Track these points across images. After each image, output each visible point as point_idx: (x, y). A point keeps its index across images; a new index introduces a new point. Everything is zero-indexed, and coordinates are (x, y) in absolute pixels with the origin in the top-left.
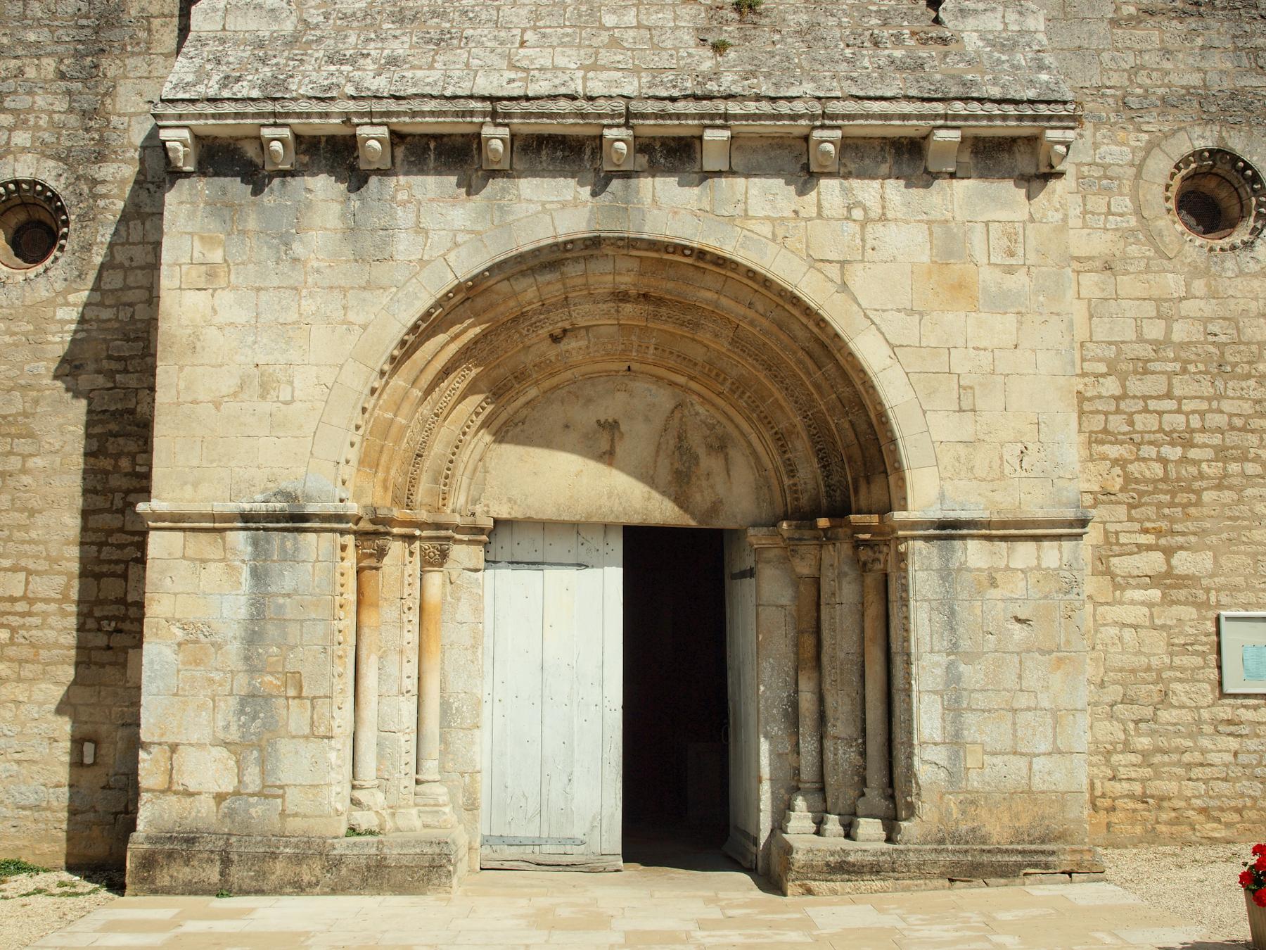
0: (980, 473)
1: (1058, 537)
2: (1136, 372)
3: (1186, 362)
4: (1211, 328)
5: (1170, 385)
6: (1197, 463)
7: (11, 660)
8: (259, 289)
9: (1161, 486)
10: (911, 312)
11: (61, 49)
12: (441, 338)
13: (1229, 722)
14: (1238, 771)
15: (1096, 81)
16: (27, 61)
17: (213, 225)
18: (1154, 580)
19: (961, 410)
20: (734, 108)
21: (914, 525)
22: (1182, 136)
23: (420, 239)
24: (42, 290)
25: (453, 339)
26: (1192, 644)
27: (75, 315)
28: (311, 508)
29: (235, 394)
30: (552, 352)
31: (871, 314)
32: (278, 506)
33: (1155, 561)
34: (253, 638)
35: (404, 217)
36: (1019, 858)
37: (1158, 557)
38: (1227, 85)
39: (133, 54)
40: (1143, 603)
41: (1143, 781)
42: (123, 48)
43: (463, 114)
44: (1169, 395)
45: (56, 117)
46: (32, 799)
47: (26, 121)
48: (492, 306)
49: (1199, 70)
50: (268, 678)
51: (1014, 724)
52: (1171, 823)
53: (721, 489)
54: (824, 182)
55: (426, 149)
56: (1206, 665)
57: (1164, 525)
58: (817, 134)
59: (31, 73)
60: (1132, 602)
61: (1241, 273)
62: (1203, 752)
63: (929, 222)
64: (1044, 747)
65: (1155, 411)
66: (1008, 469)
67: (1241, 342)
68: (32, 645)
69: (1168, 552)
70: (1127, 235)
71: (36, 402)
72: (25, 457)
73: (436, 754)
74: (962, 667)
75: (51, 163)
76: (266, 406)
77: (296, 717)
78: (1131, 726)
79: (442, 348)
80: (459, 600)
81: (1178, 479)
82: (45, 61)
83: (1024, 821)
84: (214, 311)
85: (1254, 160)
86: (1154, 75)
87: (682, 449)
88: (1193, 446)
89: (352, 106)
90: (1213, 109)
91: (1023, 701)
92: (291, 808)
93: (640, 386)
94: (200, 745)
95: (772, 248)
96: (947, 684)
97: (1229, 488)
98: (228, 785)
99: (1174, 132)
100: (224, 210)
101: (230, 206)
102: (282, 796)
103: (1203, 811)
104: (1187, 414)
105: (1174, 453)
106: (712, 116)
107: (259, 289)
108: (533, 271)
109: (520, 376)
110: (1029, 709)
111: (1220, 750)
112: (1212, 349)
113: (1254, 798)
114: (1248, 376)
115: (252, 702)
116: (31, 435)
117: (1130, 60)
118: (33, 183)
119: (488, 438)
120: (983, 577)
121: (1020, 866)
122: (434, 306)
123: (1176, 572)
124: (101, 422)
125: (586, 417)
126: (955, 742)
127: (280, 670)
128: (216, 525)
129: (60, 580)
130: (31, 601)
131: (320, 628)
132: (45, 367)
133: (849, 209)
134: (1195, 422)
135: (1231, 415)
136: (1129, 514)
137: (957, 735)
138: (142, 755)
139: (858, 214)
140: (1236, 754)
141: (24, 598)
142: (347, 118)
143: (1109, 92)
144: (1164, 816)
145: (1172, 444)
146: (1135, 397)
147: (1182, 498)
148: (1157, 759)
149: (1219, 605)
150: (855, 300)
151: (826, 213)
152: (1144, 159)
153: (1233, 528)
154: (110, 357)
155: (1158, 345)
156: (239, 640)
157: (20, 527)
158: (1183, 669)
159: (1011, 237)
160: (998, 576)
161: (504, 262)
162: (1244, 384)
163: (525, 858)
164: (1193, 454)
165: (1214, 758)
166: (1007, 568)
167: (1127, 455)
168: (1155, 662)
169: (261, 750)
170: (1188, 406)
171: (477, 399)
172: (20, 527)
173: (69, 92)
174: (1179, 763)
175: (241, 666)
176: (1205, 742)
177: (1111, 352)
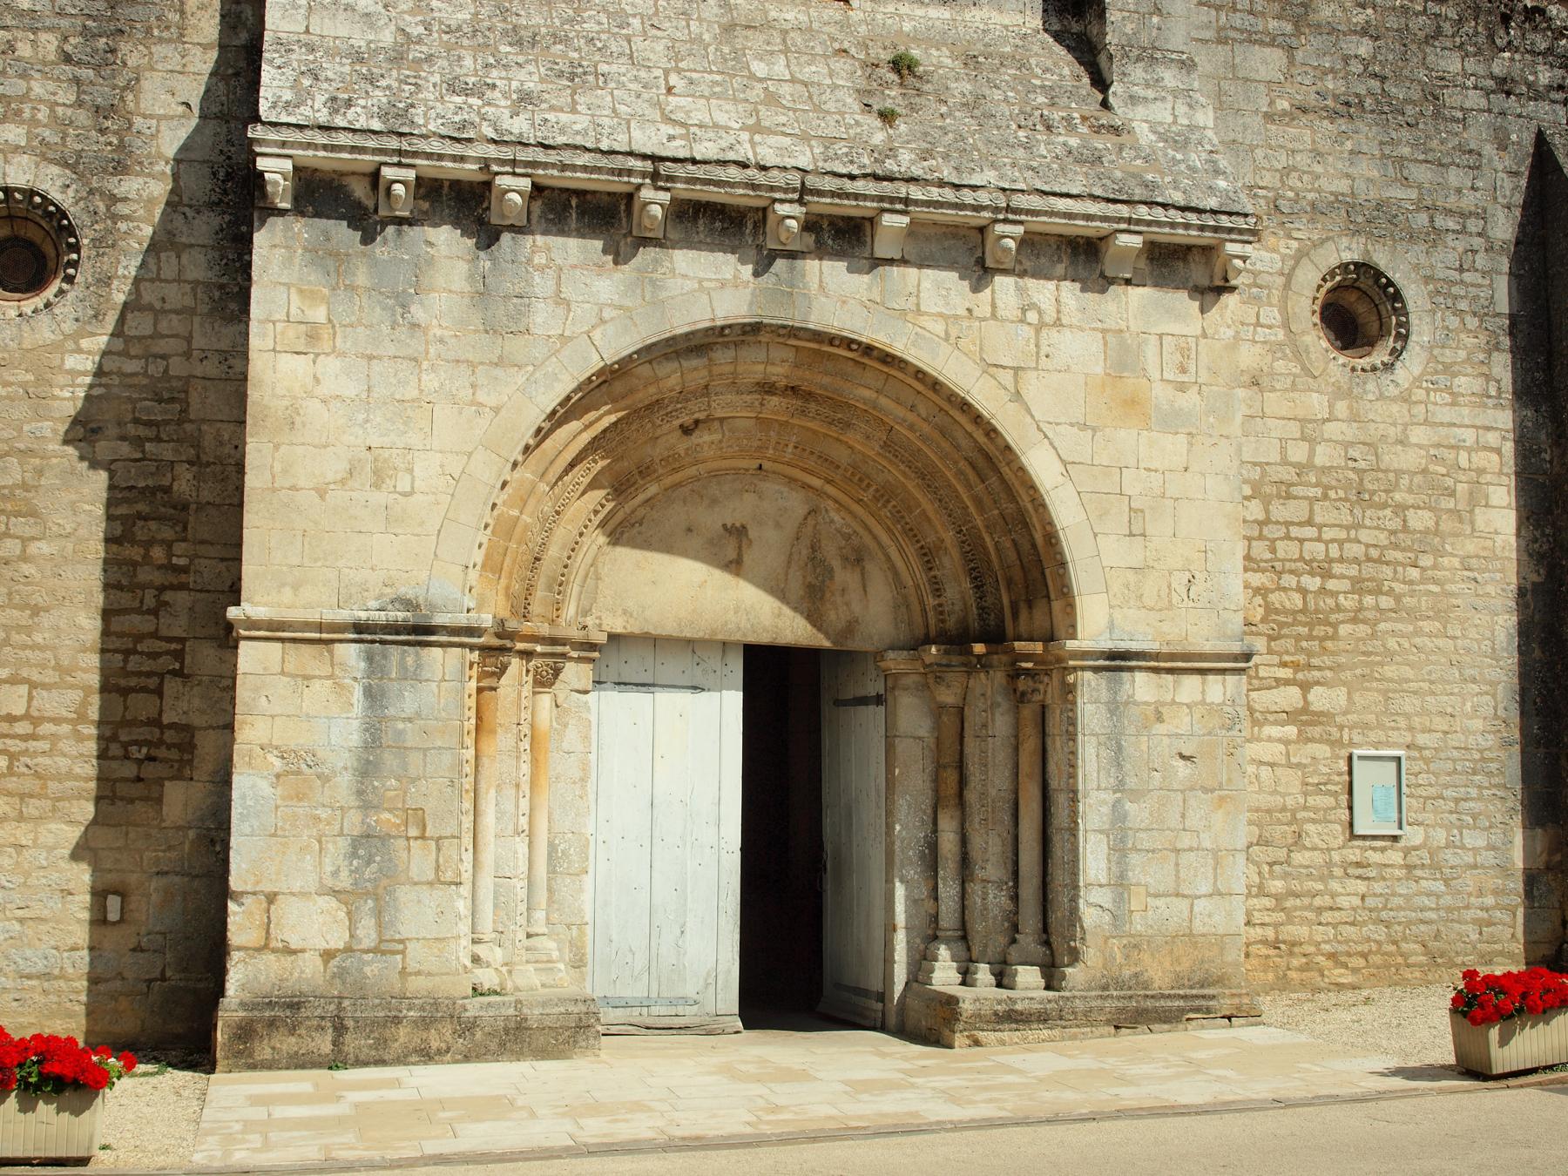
0: (1149, 602)
1: (1223, 671)
2: (1279, 497)
3: (1327, 488)
4: (1352, 453)
5: (1311, 511)
6: (1334, 594)
7: (9, 794)
8: (371, 358)
9: (1301, 617)
10: (1084, 426)
11: (64, 23)
12: (575, 425)
13: (1358, 865)
14: (1365, 915)
15: (1249, 180)
16: (20, 34)
17: (314, 277)
18: (1291, 716)
19: (1131, 535)
20: (916, 193)
21: (1084, 655)
22: (1330, 246)
23: (561, 311)
24: (45, 330)
25: (587, 427)
26: (1325, 784)
27: (89, 364)
28: (440, 619)
29: (343, 482)
30: (683, 445)
31: (1044, 427)
32: (400, 616)
33: (1290, 697)
34: (367, 769)
35: (542, 284)
36: (1181, 1003)
37: (1295, 691)
38: (1373, 194)
39: (161, 40)
40: (1280, 740)
41: (1276, 925)
42: (149, 31)
43: (620, 172)
44: (1310, 522)
45: (60, 110)
46: (40, 966)
47: (19, 113)
48: (632, 391)
49: (1348, 176)
50: (386, 816)
51: (1177, 865)
52: (1301, 969)
53: (857, 608)
54: (999, 280)
55: (567, 206)
56: (1338, 806)
57: (1302, 658)
58: (1000, 228)
59: (24, 50)
60: (1270, 739)
61: (1381, 397)
62: (1333, 895)
63: (1104, 331)
64: (1205, 888)
65: (1297, 539)
66: (1175, 599)
67: (1379, 470)
68: (37, 775)
69: (1305, 687)
70: (1274, 349)
71: (40, 472)
72: (25, 541)
73: (544, 905)
74: (1128, 806)
75: (55, 170)
76: (380, 498)
77: (419, 861)
78: (1266, 868)
79: (576, 435)
80: (566, 725)
81: (1317, 611)
82: (43, 37)
83: (1185, 965)
84: (317, 380)
85: (1396, 277)
86: (1305, 177)
87: (816, 560)
88: (1331, 576)
89: (492, 151)
90: (1360, 219)
91: (1186, 841)
92: (412, 966)
93: (770, 487)
94: (304, 894)
95: (945, 349)
96: (1113, 823)
97: (1364, 622)
98: (338, 940)
99: (1323, 241)
100: (327, 259)
101: (335, 255)
102: (403, 952)
103: (1332, 956)
104: (1327, 543)
105: (1312, 583)
106: (892, 200)
107: (371, 358)
108: (678, 354)
109: (645, 471)
110: (1191, 849)
111: (1349, 892)
112: (1352, 475)
113: (1378, 943)
114: (1384, 506)
115: (367, 844)
116: (33, 513)
117: (1282, 160)
118: (32, 193)
119: (602, 540)
120: (1150, 711)
121: (1182, 1011)
122: (575, 391)
123: (1312, 708)
124: (126, 500)
125: (711, 520)
126: (1120, 883)
127: (400, 806)
128: (322, 636)
129: (75, 696)
130: (36, 721)
131: (447, 759)
132: (52, 429)
133: (1024, 311)
134: (1334, 551)
135: (1368, 546)
136: (1269, 647)
137: (1122, 876)
138: (232, 906)
139: (1032, 316)
140: (1363, 898)
141: (27, 716)
142: (485, 164)
143: (1261, 192)
144: (1295, 962)
145: (1312, 574)
146: (1277, 523)
147: (1319, 631)
148: (1290, 903)
149: (1351, 744)
150: (1028, 411)
151: (1000, 313)
152: (1293, 269)
153: (1366, 664)
154: (136, 421)
155: (1301, 469)
156: (350, 771)
157: (19, 628)
158: (1316, 810)
159: (1184, 352)
160: (1164, 710)
161: (654, 344)
162: (1381, 513)
163: (632, 1021)
164: (1332, 585)
165: (1343, 902)
166: (1173, 702)
167: (1268, 584)
168: (1290, 802)
169: (377, 899)
170: (1328, 534)
171: (599, 494)
172: (19, 628)
173: (77, 81)
174: (1309, 908)
175: (353, 801)
176: (1335, 886)
177: (1256, 474)
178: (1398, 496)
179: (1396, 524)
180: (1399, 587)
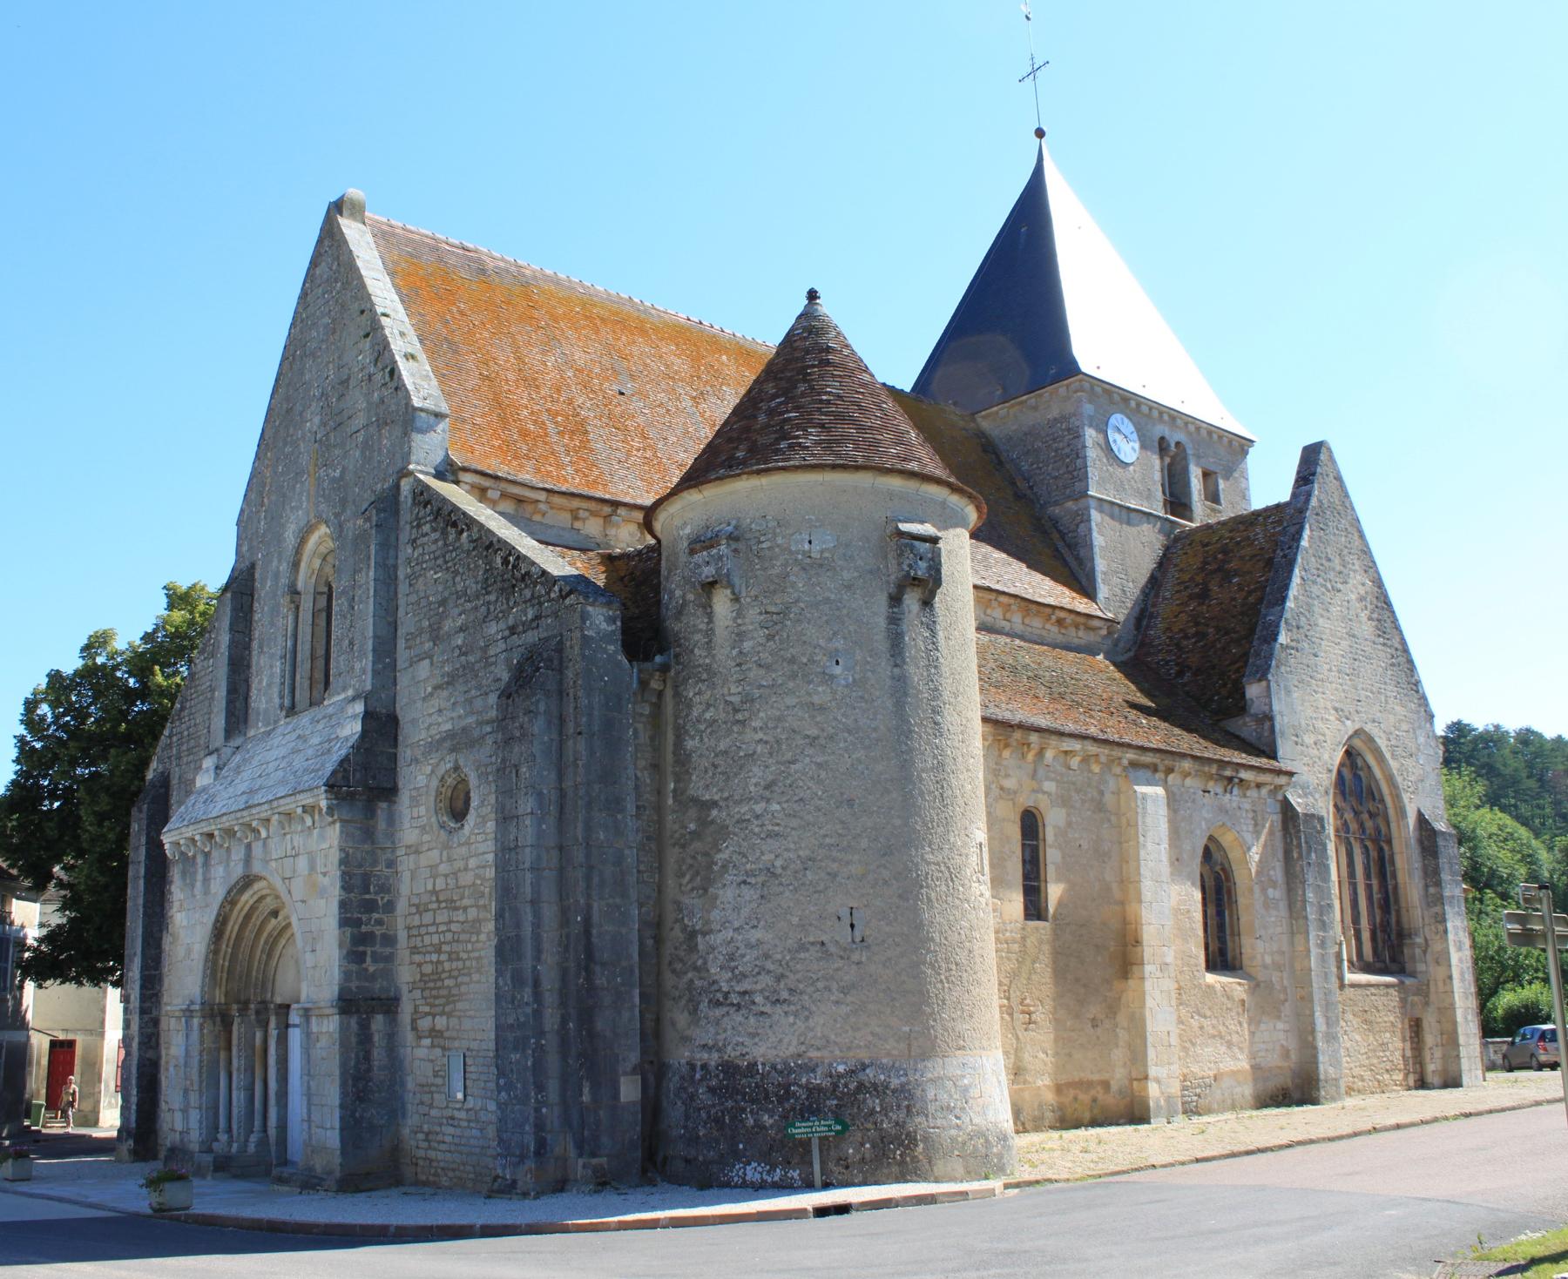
44: (434, 923)
61: (460, 845)
64: (328, 1126)
69: (434, 1016)
103: (443, 1169)
105: (434, 957)
117: (429, 721)
158: (437, 1086)
165: (448, 1139)
178: (466, 902)
179: (462, 918)
180: (464, 956)
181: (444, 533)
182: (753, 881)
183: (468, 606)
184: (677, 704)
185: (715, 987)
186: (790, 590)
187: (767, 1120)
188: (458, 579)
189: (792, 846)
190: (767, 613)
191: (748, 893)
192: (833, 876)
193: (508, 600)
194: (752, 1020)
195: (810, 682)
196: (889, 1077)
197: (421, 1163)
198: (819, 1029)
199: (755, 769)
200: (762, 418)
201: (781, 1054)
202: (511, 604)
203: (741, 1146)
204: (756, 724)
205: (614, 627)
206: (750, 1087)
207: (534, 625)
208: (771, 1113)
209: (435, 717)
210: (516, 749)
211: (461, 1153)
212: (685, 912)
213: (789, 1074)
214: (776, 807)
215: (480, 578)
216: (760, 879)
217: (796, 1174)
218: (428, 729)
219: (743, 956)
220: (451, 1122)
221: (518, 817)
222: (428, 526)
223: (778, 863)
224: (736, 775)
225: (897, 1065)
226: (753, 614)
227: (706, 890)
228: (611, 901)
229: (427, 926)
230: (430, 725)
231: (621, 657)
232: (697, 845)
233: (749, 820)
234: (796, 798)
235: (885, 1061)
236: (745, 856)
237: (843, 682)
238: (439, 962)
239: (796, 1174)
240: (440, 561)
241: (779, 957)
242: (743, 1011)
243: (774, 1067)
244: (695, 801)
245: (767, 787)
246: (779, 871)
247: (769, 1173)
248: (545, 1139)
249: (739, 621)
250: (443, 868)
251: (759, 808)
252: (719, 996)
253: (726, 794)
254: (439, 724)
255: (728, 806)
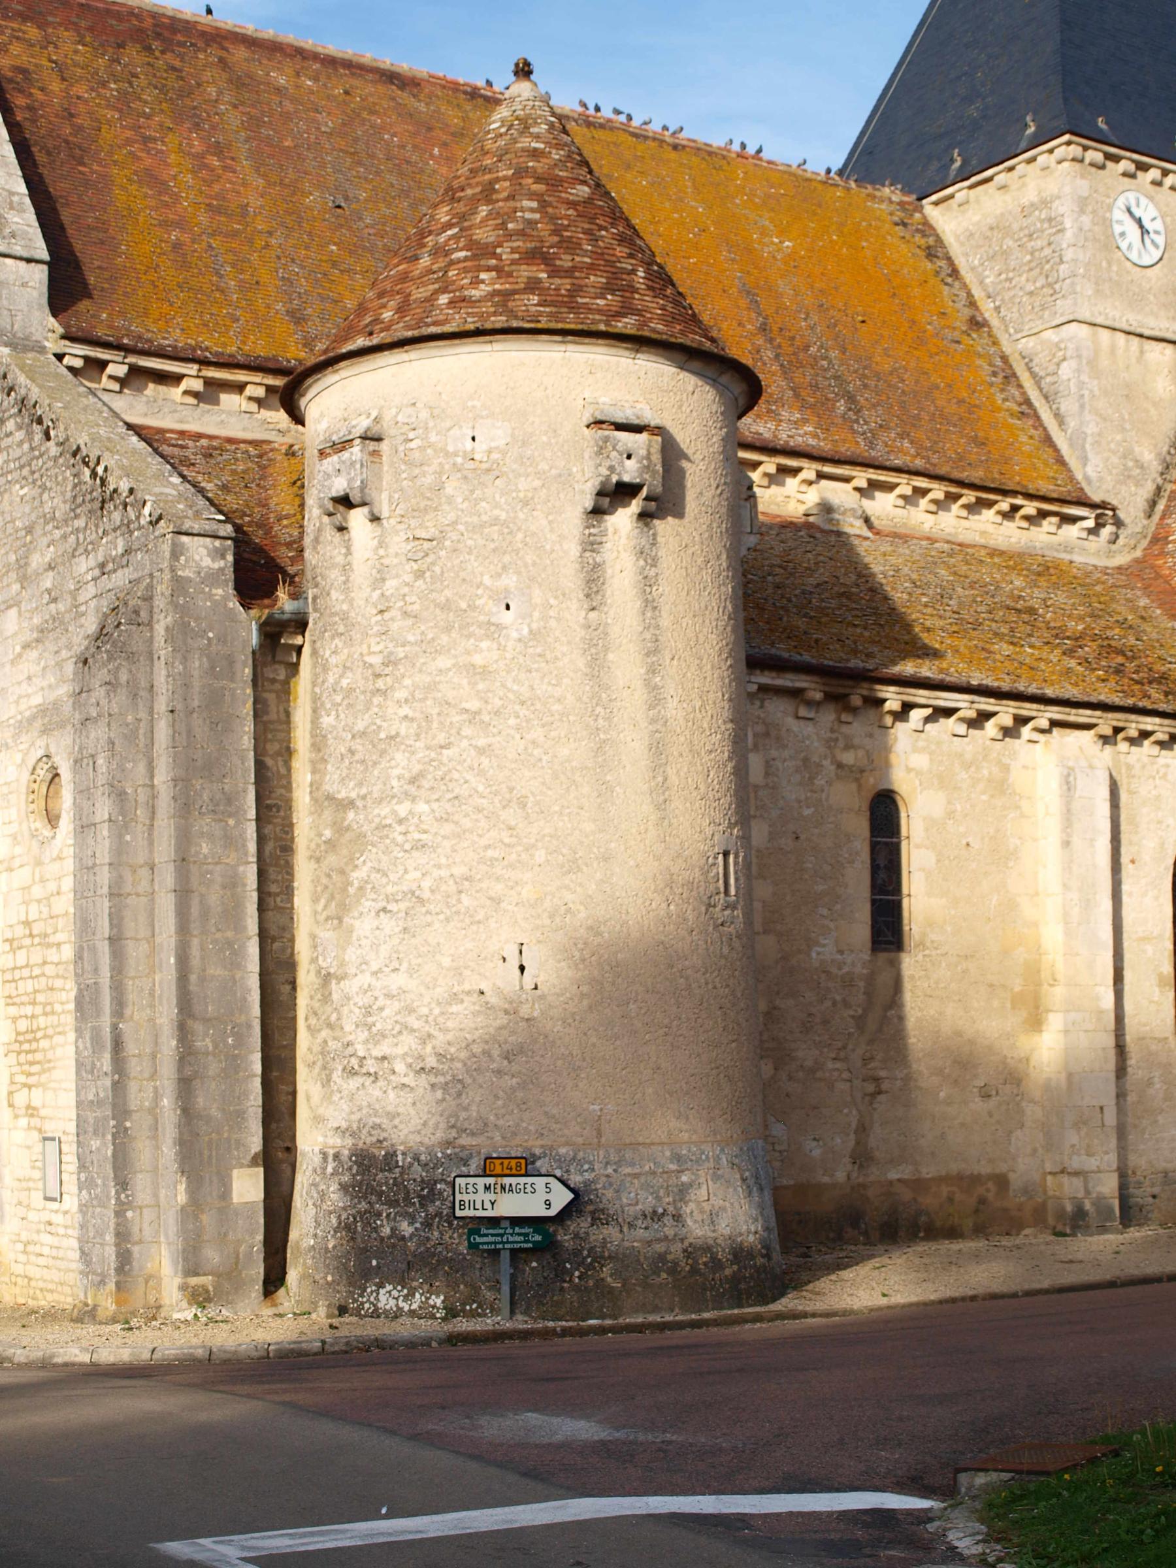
44: (27, 966)
69: (30, 1087)
103: (41, 1290)
105: (29, 1010)
165: (46, 1251)
179: (56, 959)
181: (30, 434)
182: (392, 907)
183: (57, 534)
184: (314, 666)
185: (350, 1050)
186: (446, 507)
187: (406, 1228)
188: (46, 496)
189: (443, 861)
190: (416, 539)
191: (389, 925)
192: (496, 901)
193: (97, 526)
194: (392, 1095)
195: (469, 636)
196: (568, 1171)
197: (19, 1280)
198: (474, 1108)
199: (399, 756)
200: (425, 261)
201: (426, 1141)
202: (100, 532)
203: (374, 1263)
204: (401, 694)
205: (222, 563)
206: (386, 1184)
207: (124, 562)
208: (412, 1220)
209: (24, 685)
210: (93, 735)
211: (59, 1270)
212: (320, 949)
213: (435, 1167)
214: (422, 807)
215: (69, 495)
216: (403, 906)
217: (438, 1301)
218: (17, 702)
219: (381, 1009)
220: (49, 1228)
221: (95, 825)
222: (12, 421)
223: (427, 884)
224: (375, 763)
225: (581, 1155)
226: (398, 543)
227: (340, 920)
228: (218, 935)
229: (22, 967)
230: (20, 697)
231: (234, 604)
232: (332, 860)
233: (390, 825)
234: (450, 796)
235: (563, 1151)
236: (385, 875)
237: (515, 635)
238: (33, 1016)
239: (438, 1301)
240: (26, 472)
241: (425, 1011)
242: (381, 1083)
243: (416, 1158)
244: (330, 798)
245: (413, 781)
246: (426, 895)
247: (406, 1299)
248: (128, 1251)
249: (381, 552)
250: (37, 892)
251: (403, 809)
252: (354, 1062)
253: (364, 791)
254: (28, 696)
255: (365, 807)
